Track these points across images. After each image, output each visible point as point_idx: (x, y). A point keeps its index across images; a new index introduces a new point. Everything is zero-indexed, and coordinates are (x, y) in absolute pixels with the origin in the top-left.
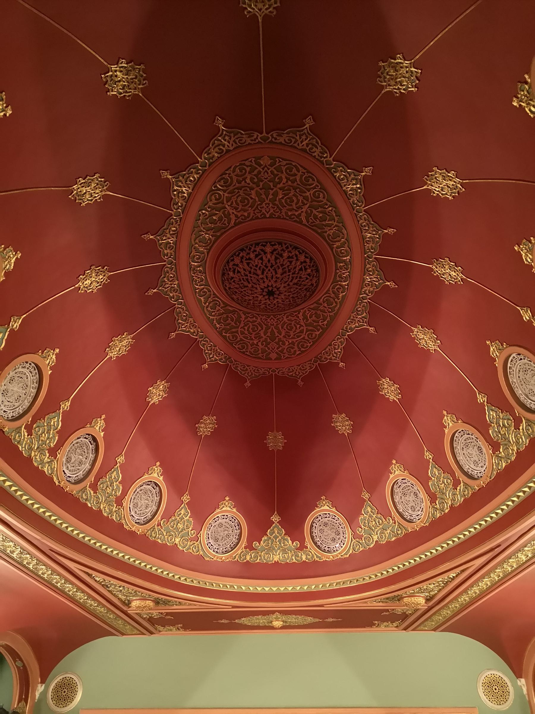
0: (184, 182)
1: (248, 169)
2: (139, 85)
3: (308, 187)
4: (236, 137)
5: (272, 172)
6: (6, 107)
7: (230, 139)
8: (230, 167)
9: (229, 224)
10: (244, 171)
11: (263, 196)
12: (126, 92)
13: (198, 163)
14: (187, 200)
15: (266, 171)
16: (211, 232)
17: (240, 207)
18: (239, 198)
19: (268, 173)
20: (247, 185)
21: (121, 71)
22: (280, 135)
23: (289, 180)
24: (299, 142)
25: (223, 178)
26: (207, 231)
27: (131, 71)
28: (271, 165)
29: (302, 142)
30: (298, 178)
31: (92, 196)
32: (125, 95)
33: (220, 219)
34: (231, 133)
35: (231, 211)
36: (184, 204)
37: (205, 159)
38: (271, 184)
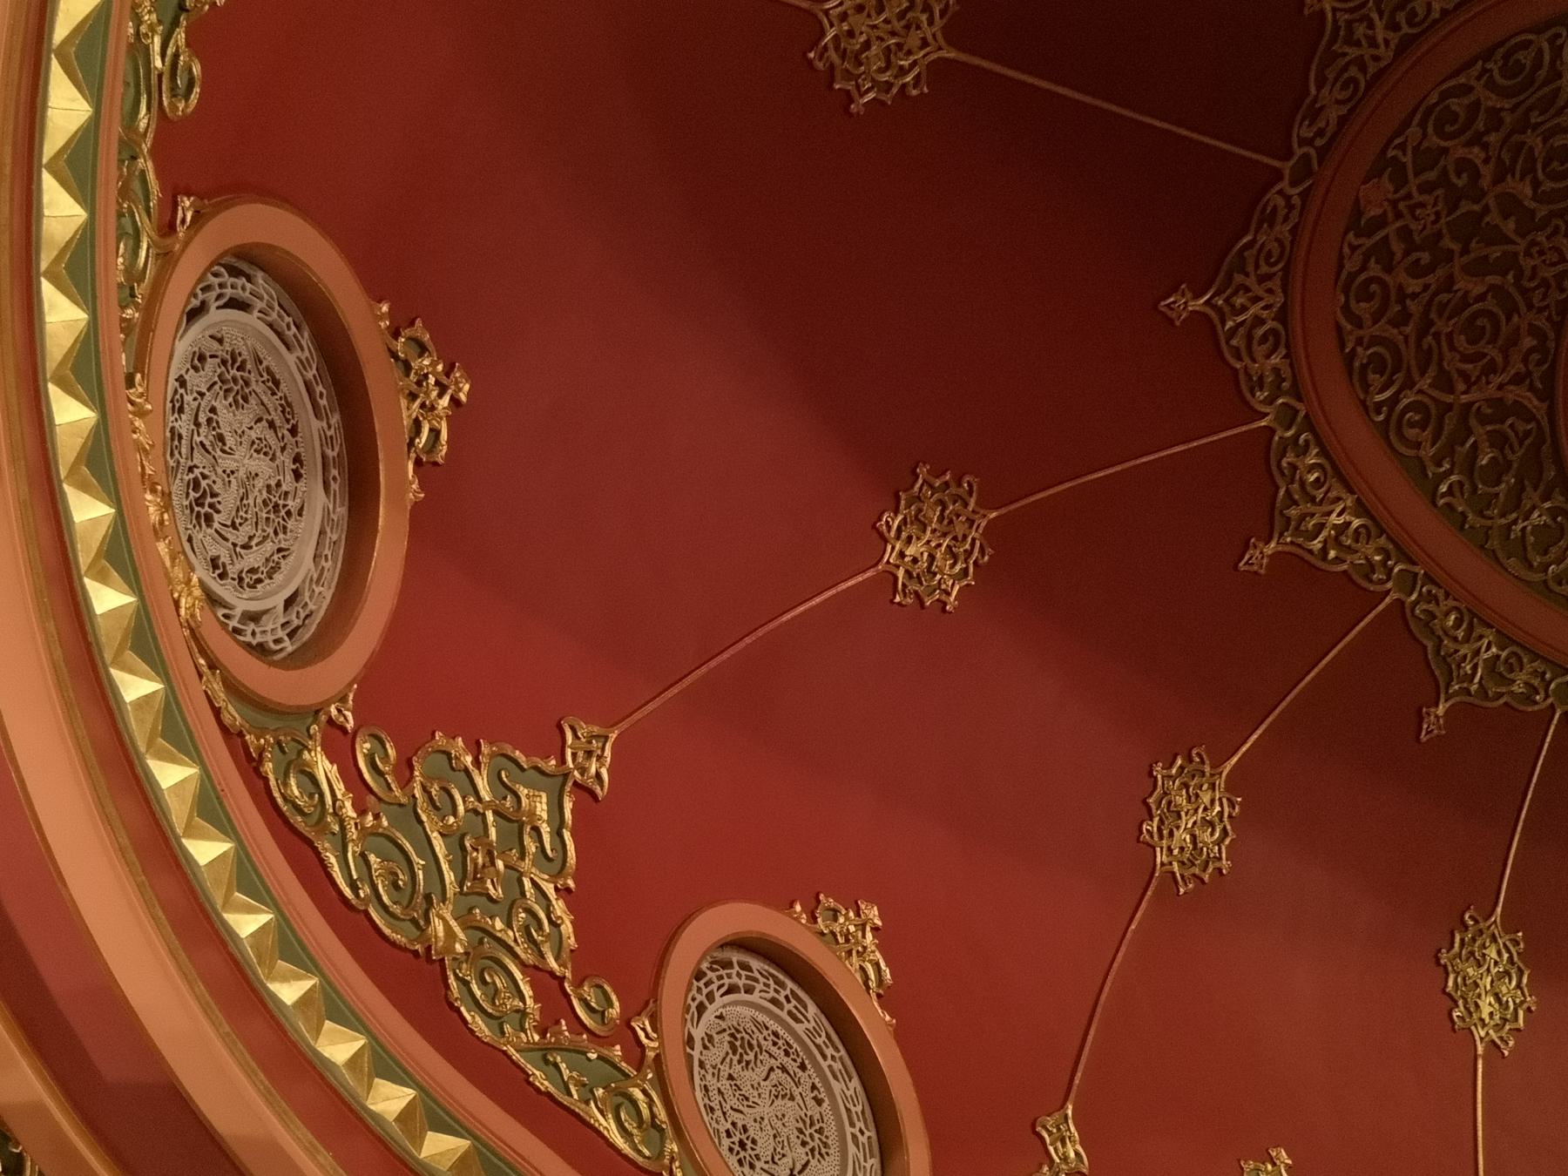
0: (1310, 507)
1: (1375, 270)
2: (966, 505)
3: (1542, 73)
4: (1250, 268)
5: (1426, 188)
6: (858, 914)
7: (1247, 290)
8: (1339, 328)
9: (1531, 418)
10: (1374, 287)
11: (1496, 252)
12: (969, 553)
13: (1272, 431)
14: (1376, 526)
15: (1412, 209)
16: (1531, 497)
17: (1493, 352)
18: (1461, 341)
19: (1422, 205)
20: (1426, 296)
21: (909, 540)
22: (1315, 114)
23: (1487, 132)
24: (1366, 52)
25: (1364, 367)
26: (1517, 507)
27: (920, 510)
28: (1400, 180)
29: (1373, 43)
30: (1493, 101)
31: (1211, 824)
32: (975, 563)
33: (1499, 441)
34: (1229, 278)
35: (1491, 391)
36: (1383, 540)
37: (1270, 401)
38: (1466, 207)
